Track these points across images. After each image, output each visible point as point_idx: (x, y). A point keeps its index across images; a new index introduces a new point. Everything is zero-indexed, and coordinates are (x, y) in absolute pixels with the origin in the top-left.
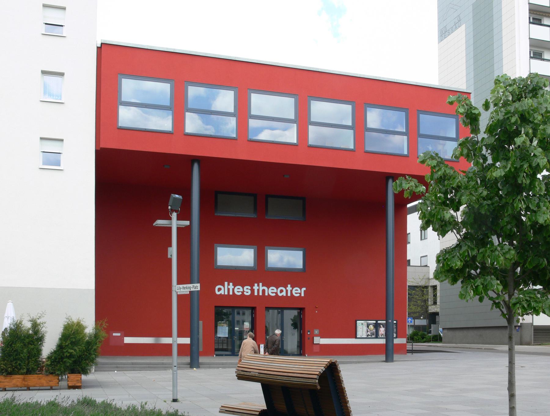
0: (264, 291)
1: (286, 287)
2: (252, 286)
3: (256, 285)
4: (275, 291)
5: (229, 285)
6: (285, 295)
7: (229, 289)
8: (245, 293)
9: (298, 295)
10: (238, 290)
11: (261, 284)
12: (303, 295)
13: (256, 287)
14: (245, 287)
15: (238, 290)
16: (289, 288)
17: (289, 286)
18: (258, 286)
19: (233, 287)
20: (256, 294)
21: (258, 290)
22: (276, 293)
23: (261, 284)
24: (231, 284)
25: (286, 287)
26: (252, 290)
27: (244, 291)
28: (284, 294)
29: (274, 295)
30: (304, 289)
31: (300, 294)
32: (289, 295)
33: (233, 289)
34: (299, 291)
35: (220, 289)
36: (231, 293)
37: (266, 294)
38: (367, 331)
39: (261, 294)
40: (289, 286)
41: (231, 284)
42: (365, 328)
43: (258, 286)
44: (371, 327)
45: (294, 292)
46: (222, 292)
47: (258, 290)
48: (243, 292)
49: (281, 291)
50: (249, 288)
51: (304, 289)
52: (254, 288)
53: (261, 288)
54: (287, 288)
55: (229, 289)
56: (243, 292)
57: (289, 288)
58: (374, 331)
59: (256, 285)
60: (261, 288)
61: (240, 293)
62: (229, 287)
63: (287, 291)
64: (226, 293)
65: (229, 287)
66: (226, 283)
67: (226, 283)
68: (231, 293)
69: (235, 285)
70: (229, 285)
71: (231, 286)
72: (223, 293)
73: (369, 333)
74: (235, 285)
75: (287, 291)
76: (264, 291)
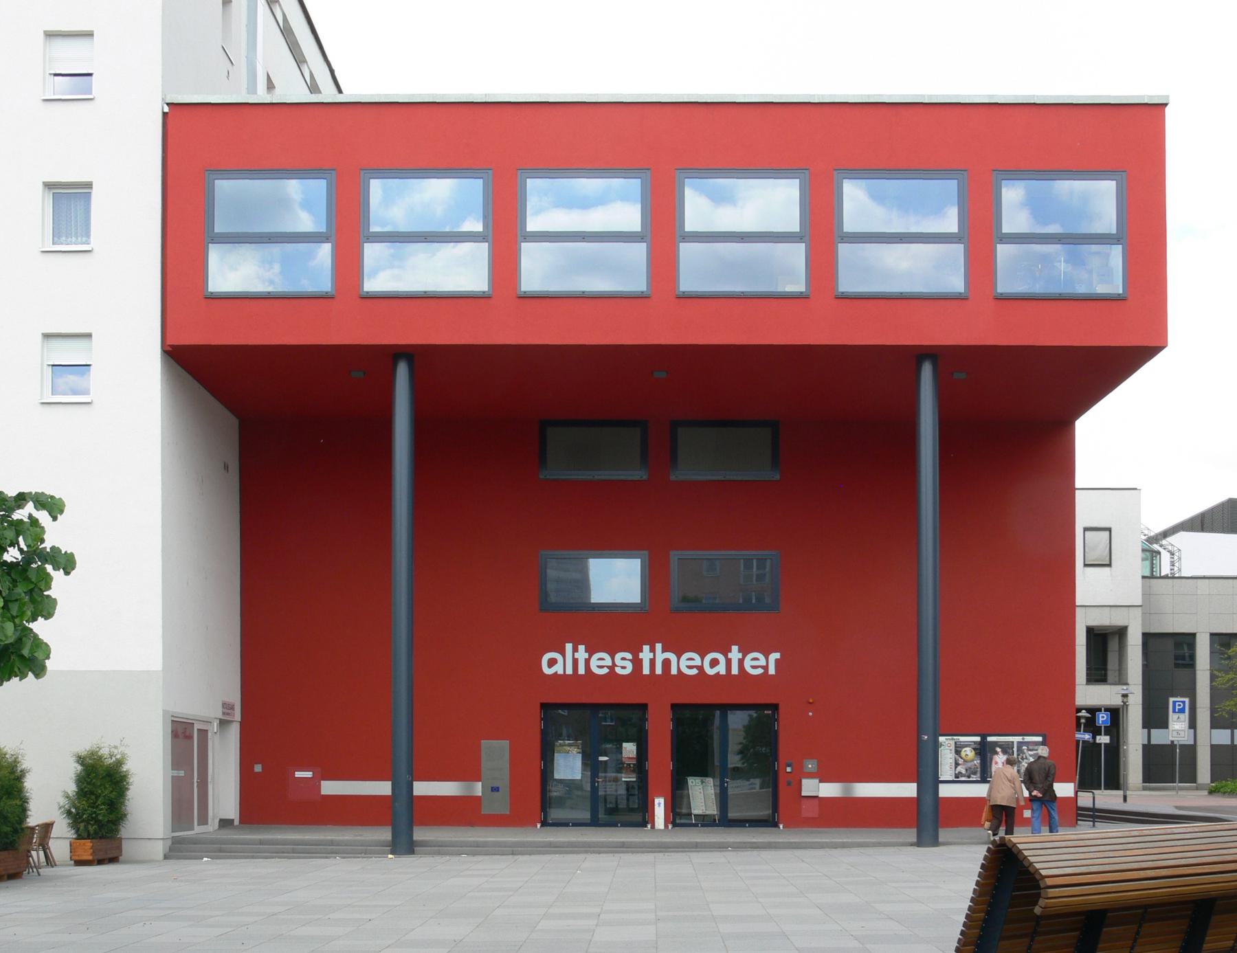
0: (666, 663)
2: (636, 651)
3: (646, 648)
5: (575, 650)
7: (575, 662)
8: (618, 670)
9: (760, 671)
10: (600, 663)
11: (659, 646)
13: (646, 655)
15: (600, 663)
18: (653, 650)
20: (646, 671)
21: (653, 662)
26: (637, 663)
30: (775, 656)
31: (766, 668)
34: (762, 662)
35: (552, 662)
37: (674, 671)
38: (957, 764)
39: (659, 671)
40: (735, 648)
41: (582, 648)
43: (653, 650)
45: (748, 664)
46: (558, 669)
47: (653, 662)
50: (629, 656)
51: (775, 656)
52: (641, 655)
55: (575, 662)
56: (612, 668)
60: (660, 657)
61: (606, 671)
64: (569, 671)
67: (569, 647)
69: (591, 651)
70: (575, 650)
73: (961, 769)
74: (591, 651)
76: (666, 663)
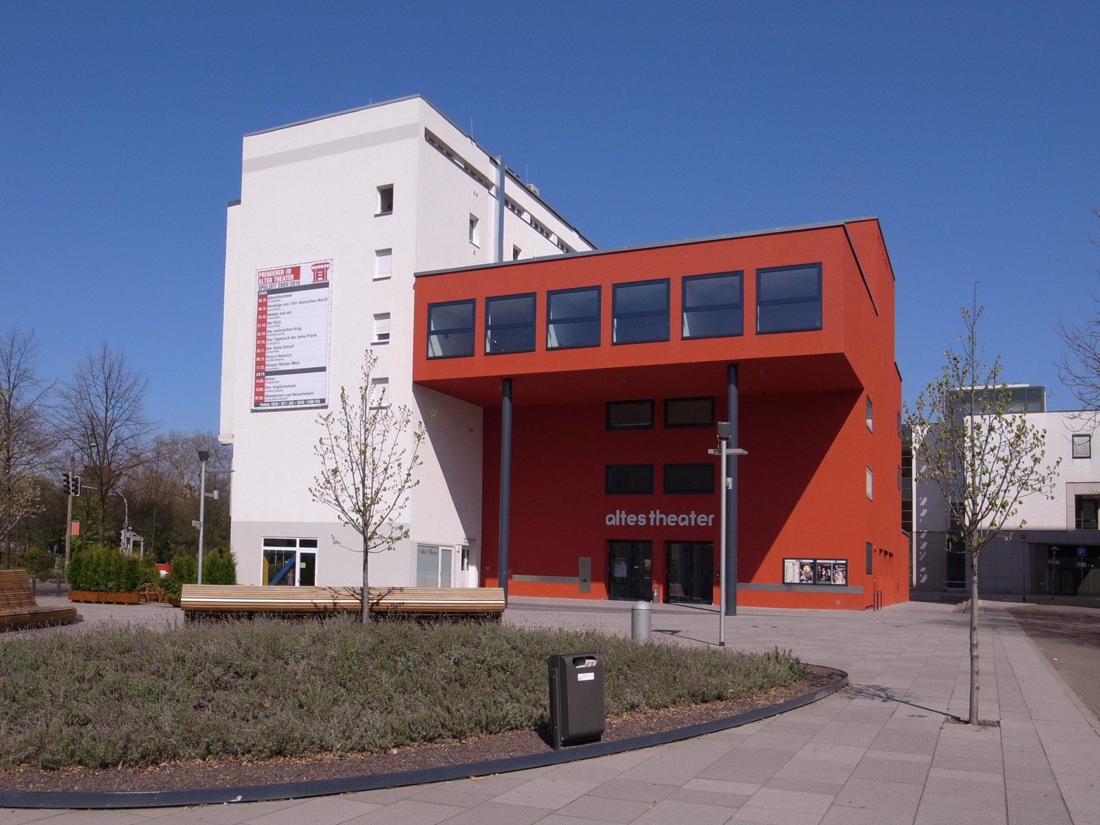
0: (661, 519)
1: (688, 514)
2: (647, 514)
3: (652, 512)
4: (675, 519)
5: (621, 513)
6: (687, 524)
7: (621, 519)
8: (639, 523)
9: (704, 524)
10: (631, 520)
11: (658, 511)
12: (710, 524)
13: (652, 516)
14: (640, 516)
15: (631, 520)
16: (693, 515)
17: (693, 512)
18: (655, 513)
19: (626, 516)
20: (652, 524)
21: (655, 519)
22: (677, 522)
23: (658, 511)
24: (623, 512)
25: (688, 514)
26: (648, 520)
27: (638, 520)
28: (686, 523)
29: (674, 524)
31: (707, 522)
32: (693, 524)
33: (626, 519)
34: (706, 519)
35: (610, 519)
36: (623, 524)
37: (665, 524)
38: (801, 575)
39: (658, 524)
40: (693, 512)
41: (623, 512)
42: (797, 570)
43: (655, 513)
44: (807, 568)
45: (699, 520)
46: (613, 522)
47: (655, 519)
48: (637, 522)
49: (683, 520)
53: (659, 516)
54: (691, 516)
55: (621, 519)
56: (637, 522)
57: (693, 515)
58: (812, 574)
59: (652, 512)
62: (621, 516)
63: (690, 519)
64: (618, 524)
65: (621, 516)
66: (618, 511)
67: (618, 511)
68: (623, 524)
69: (627, 514)
70: (621, 513)
71: (624, 515)
72: (614, 524)
74: (627, 514)
75: (690, 519)
76: (661, 519)
